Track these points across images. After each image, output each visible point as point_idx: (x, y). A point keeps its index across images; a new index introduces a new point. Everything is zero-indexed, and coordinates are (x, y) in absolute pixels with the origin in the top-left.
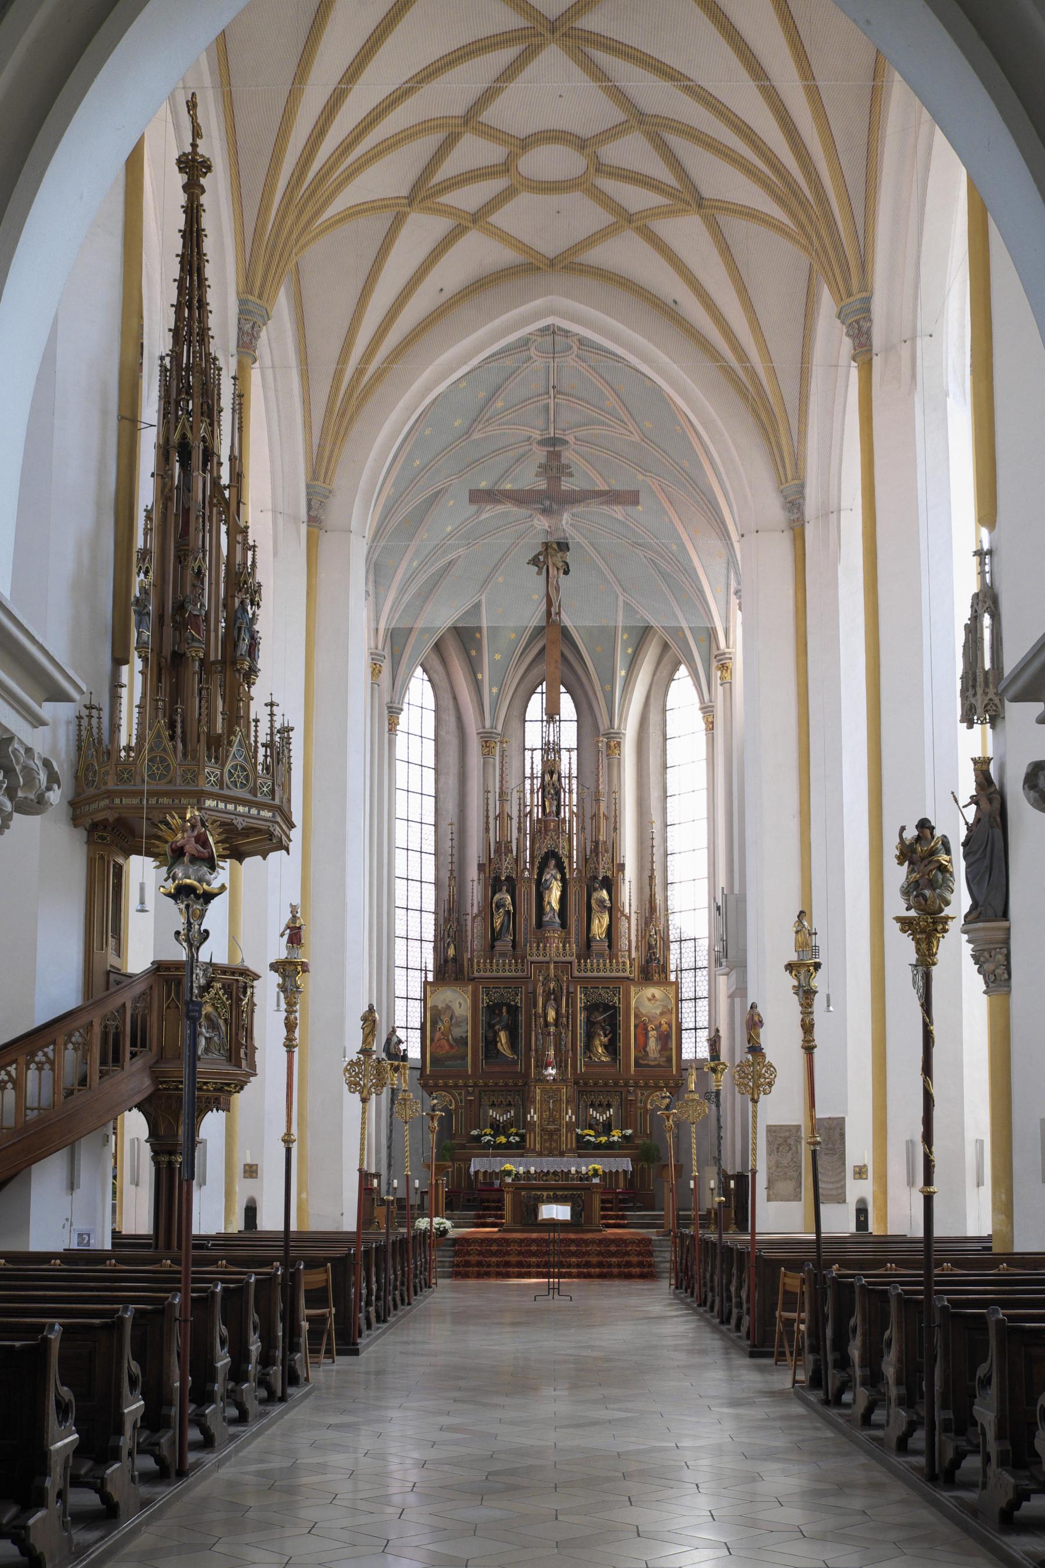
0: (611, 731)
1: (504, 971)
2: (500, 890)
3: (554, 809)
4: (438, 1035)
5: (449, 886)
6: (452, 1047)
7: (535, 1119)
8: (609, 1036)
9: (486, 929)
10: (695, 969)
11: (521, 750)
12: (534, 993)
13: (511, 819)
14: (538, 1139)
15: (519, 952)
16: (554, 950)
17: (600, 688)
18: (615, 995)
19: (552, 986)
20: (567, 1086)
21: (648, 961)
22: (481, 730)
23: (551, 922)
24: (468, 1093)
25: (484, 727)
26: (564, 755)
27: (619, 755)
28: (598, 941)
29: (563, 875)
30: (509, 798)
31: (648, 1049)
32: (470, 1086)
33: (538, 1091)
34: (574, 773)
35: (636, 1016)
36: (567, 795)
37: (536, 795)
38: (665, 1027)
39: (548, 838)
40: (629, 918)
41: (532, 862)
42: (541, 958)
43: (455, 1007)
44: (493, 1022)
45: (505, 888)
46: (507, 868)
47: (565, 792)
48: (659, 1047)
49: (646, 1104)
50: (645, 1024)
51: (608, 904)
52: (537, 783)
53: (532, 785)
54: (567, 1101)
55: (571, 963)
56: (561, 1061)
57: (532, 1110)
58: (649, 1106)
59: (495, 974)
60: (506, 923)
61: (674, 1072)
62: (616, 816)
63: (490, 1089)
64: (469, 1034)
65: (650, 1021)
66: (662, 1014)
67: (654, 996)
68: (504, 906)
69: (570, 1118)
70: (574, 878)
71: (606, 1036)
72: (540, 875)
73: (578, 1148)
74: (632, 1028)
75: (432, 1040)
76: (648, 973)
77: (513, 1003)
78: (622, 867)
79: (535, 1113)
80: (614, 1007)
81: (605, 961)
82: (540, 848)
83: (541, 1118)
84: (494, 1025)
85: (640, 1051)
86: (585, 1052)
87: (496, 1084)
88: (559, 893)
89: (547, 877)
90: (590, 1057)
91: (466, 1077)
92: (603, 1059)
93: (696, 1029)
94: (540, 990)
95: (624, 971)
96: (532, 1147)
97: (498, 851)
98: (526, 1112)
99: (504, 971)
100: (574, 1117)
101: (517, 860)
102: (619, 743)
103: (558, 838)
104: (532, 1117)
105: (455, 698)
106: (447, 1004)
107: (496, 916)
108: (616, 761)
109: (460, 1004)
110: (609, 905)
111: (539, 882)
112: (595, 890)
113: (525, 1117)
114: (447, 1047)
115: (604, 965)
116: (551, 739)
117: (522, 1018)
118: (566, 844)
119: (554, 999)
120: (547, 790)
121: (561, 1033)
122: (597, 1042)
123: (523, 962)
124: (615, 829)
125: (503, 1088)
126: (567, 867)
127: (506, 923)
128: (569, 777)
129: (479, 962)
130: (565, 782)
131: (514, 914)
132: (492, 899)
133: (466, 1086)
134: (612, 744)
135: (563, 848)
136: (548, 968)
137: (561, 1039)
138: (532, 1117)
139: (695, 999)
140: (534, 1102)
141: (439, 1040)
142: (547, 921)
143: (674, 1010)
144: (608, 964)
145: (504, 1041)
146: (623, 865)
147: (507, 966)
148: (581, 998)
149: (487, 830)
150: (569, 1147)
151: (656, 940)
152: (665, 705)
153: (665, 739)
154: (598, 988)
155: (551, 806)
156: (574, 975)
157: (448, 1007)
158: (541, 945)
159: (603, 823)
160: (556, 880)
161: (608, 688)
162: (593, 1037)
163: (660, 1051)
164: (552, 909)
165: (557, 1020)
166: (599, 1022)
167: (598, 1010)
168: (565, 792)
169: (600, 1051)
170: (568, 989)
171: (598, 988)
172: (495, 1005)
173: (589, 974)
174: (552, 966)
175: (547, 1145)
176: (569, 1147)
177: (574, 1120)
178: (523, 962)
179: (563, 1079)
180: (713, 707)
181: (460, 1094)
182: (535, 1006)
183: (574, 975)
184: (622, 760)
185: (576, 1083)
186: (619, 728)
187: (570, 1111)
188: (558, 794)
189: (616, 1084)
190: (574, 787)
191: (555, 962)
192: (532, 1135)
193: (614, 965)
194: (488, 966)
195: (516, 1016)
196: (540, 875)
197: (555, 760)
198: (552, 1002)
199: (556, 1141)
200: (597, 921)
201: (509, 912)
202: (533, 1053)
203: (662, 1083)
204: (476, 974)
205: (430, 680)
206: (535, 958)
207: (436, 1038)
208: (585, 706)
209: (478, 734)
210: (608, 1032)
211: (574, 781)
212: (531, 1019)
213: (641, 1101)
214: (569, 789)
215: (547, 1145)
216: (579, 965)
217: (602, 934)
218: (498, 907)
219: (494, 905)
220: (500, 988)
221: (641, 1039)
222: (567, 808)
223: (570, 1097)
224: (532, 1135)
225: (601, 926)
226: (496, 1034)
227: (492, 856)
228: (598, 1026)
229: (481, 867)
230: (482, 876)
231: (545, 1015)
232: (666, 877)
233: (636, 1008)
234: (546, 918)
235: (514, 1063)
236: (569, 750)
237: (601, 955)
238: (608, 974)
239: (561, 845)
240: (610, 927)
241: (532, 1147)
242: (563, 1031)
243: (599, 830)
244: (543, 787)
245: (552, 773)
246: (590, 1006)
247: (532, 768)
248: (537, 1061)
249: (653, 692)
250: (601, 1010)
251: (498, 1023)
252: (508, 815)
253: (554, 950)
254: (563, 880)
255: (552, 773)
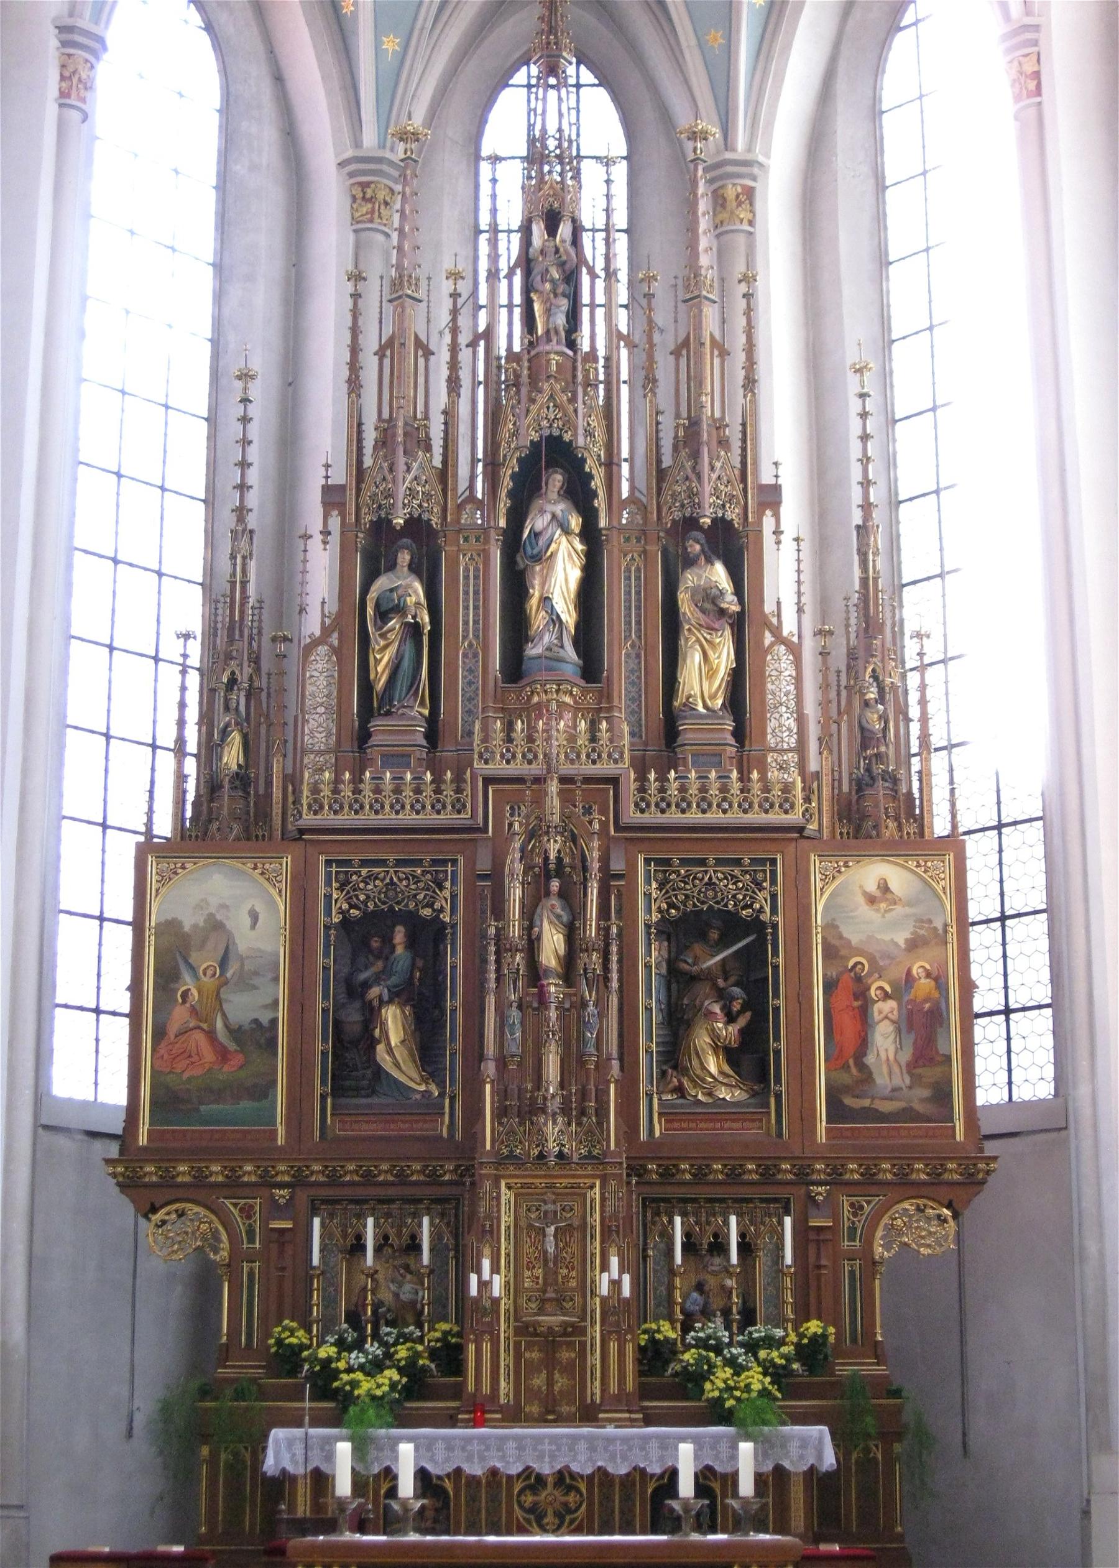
0: (728, 155)
1: (398, 806)
2: (392, 566)
3: (561, 320)
4: (179, 1016)
5: (233, 557)
6: (223, 1055)
7: (497, 1290)
8: (742, 1021)
9: (342, 684)
10: (999, 827)
11: (469, 233)
12: (496, 876)
13: (428, 353)
14: (505, 1360)
15: (447, 752)
16: (559, 740)
17: (693, 42)
18: (759, 885)
19: (553, 848)
20: (604, 1180)
21: (860, 786)
22: (349, 153)
23: (552, 658)
24: (275, 1209)
25: (357, 143)
26: (592, 174)
27: (751, 223)
28: (701, 716)
29: (589, 516)
30: (422, 294)
31: (870, 1059)
32: (281, 1186)
33: (506, 1195)
34: (621, 219)
35: (831, 953)
36: (600, 284)
37: (504, 283)
38: (924, 985)
39: (541, 399)
40: (795, 650)
41: (493, 466)
42: (517, 768)
43: (239, 923)
44: (363, 976)
45: (404, 558)
46: (411, 493)
47: (593, 276)
48: (906, 1056)
49: (869, 1242)
50: (858, 979)
51: (730, 602)
52: (510, 248)
53: (494, 257)
54: (607, 1232)
55: (614, 781)
56: (583, 1095)
57: (486, 1264)
58: (878, 1250)
59: (367, 818)
60: (406, 664)
61: (960, 1136)
62: (750, 348)
63: (347, 1192)
64: (282, 1014)
65: (877, 970)
66: (914, 945)
67: (884, 888)
68: (400, 609)
69: (616, 1284)
70: (621, 529)
71: (730, 1018)
72: (518, 515)
73: (645, 1392)
74: (818, 993)
75: (159, 1034)
76: (864, 817)
77: (427, 912)
78: (771, 497)
79: (495, 1269)
80: (757, 926)
81: (724, 777)
82: (515, 434)
83: (514, 1287)
84: (366, 985)
85: (846, 1067)
86: (663, 1074)
87: (368, 1178)
88: (575, 574)
89: (537, 521)
90: (680, 1090)
91: (265, 1153)
92: (723, 1093)
93: (1007, 1011)
94: (514, 865)
95: (787, 805)
96: (486, 1389)
97: (384, 442)
98: (465, 1263)
99: (398, 806)
100: (626, 1278)
101: (445, 474)
102: (750, 193)
103: (573, 400)
104: (483, 1285)
105: (279, 78)
106: (211, 916)
107: (377, 643)
108: (741, 239)
109: (254, 917)
110: (736, 608)
111: (513, 541)
112: (690, 562)
113: (463, 1284)
114: (209, 1056)
115: (724, 789)
116: (552, 129)
117: (455, 959)
118: (597, 423)
119: (563, 895)
120: (537, 270)
121: (584, 1004)
122: (702, 1039)
123: (458, 779)
124: (750, 383)
125: (391, 1192)
126: (601, 493)
127: (406, 664)
128: (607, 229)
129: (315, 790)
130: (593, 248)
131: (435, 635)
132: (365, 591)
133: (267, 1183)
134: (730, 192)
135: (589, 433)
136: (539, 800)
137: (582, 1023)
138: (483, 1285)
139: (1003, 918)
140: (492, 1233)
141: (183, 1032)
142: (539, 657)
143: (953, 930)
144: (735, 786)
145: (395, 1037)
146: (776, 489)
147: (408, 792)
148: (648, 896)
149: (354, 384)
150: (613, 1388)
151: (884, 718)
152: (876, 100)
153: (881, 187)
154: (702, 862)
155: (548, 312)
156: (625, 820)
157: (216, 926)
158: (519, 725)
159: (711, 366)
160: (567, 531)
161: (716, 38)
162: (689, 1025)
163: (912, 1066)
164: (556, 620)
165: (569, 961)
166: (707, 976)
167: (703, 936)
168: (593, 276)
169: (713, 1068)
170: (605, 860)
171: (702, 862)
172: (370, 918)
173: (674, 817)
174: (554, 787)
175: (539, 1381)
176: (613, 1388)
177: (626, 1292)
178: (458, 779)
179: (590, 1156)
180: (1036, 28)
181: (247, 1212)
182: (499, 912)
183: (625, 820)
184: (759, 237)
185: (636, 1169)
186: (750, 149)
187: (614, 1261)
188: (571, 278)
189: (768, 1174)
190: (621, 263)
191: (563, 780)
192: (486, 1347)
193: (756, 788)
194: (347, 792)
195: (438, 957)
196: (518, 515)
197: (562, 182)
198: (555, 901)
199: (568, 1369)
200: (697, 657)
201: (415, 630)
202: (490, 1068)
203: (920, 1172)
204: (308, 819)
205: (209, 28)
206: (498, 767)
207: (173, 1028)
208: (648, 114)
209: (342, 165)
210: (736, 1006)
211: (621, 243)
212: (485, 961)
213: (853, 1230)
214: (607, 268)
215: (539, 1381)
216: (642, 789)
217: (713, 697)
218: (383, 615)
219: (370, 611)
220: (383, 863)
221: (848, 1025)
222: (600, 313)
223: (615, 1216)
224: (486, 1347)
225: (711, 673)
226: (371, 1015)
227: (368, 462)
228: (704, 988)
229: (332, 496)
230: (335, 523)
231: (532, 946)
232: (895, 567)
233: (830, 927)
234: (533, 650)
235: (431, 1108)
236: (607, 162)
237: (710, 758)
238: (735, 817)
239: (581, 423)
240: (737, 678)
241: (486, 1389)
242: (591, 997)
243: (700, 384)
244: (526, 263)
245: (552, 221)
246: (676, 923)
247: (494, 211)
248: (502, 1094)
249: (842, 66)
250: (714, 935)
251: (377, 979)
252: (418, 343)
253: (559, 740)
254: (590, 535)
255: (552, 221)
